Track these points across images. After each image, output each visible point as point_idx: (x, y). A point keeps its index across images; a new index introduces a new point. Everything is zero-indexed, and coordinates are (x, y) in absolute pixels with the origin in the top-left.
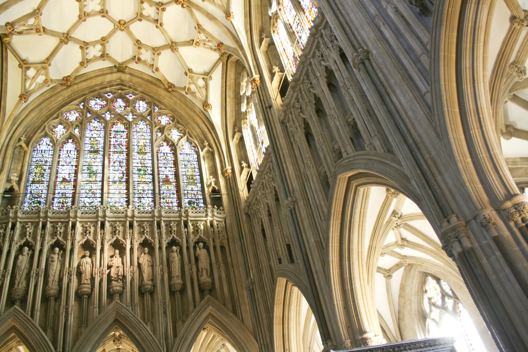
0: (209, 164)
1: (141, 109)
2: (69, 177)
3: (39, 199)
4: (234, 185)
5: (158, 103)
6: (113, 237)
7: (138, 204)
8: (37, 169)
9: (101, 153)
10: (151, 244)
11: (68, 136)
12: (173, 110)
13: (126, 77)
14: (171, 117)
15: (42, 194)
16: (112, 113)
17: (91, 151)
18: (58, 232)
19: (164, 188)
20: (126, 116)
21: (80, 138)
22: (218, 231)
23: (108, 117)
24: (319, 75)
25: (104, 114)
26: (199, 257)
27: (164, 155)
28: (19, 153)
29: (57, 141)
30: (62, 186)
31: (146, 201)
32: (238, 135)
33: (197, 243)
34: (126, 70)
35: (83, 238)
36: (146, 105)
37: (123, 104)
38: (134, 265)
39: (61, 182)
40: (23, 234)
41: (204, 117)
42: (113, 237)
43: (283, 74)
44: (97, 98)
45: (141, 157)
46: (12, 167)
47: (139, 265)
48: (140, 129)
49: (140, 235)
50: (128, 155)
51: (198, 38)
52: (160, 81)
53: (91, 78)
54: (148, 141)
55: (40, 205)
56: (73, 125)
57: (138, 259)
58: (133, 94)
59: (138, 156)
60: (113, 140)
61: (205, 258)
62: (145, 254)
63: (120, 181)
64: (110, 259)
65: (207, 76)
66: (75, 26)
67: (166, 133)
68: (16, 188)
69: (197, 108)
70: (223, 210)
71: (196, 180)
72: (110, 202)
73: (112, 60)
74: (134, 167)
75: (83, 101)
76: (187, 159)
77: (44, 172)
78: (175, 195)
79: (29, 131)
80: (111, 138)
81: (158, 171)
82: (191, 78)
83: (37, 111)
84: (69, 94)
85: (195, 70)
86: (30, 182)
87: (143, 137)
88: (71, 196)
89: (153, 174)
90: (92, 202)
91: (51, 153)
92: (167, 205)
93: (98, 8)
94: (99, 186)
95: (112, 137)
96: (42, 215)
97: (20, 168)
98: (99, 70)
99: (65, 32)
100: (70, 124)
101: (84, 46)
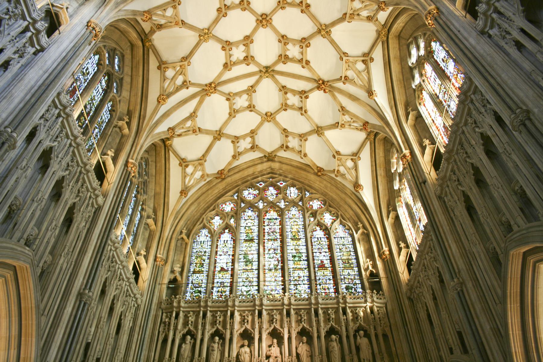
0: (364, 247)
1: (292, 195)
3: (199, 289)
4: (393, 267)
5: (308, 188)
6: (270, 326)
7: (294, 292)
9: (256, 241)
10: (309, 332)
11: (224, 227)
12: (324, 194)
13: (276, 165)
14: (322, 201)
15: (202, 283)
16: (265, 201)
18: (218, 322)
19: (319, 274)
20: (278, 204)
21: (236, 228)
22: (379, 318)
23: (261, 205)
24: (474, 143)
25: (257, 203)
26: (360, 347)
27: (318, 240)
28: (181, 245)
29: (214, 232)
30: (220, 275)
31: (302, 288)
32: (393, 214)
33: (357, 331)
34: (276, 159)
35: (242, 327)
36: (296, 191)
37: (274, 192)
38: (292, 355)
39: (220, 272)
40: (186, 324)
41: (356, 198)
42: (270, 326)
43: (434, 146)
44: (249, 188)
45: (295, 244)
46: (175, 258)
47: (298, 355)
49: (297, 324)
50: (281, 242)
51: (343, 120)
52: (309, 166)
53: (243, 170)
54: (301, 227)
55: (200, 294)
56: (228, 215)
57: (296, 348)
58: (284, 181)
60: (267, 228)
61: (367, 348)
62: (303, 343)
63: (275, 269)
64: (268, 349)
65: (356, 156)
66: (226, 123)
67: (318, 217)
68: (179, 278)
69: (348, 190)
70: (383, 295)
71: (352, 264)
72: (266, 290)
73: (262, 150)
74: (288, 254)
75: (237, 192)
76: (342, 243)
78: (332, 281)
79: (189, 224)
81: (313, 256)
82: (340, 160)
83: (196, 204)
84: (224, 186)
85: (342, 151)
86: (191, 272)
87: (296, 223)
88: (229, 285)
89: (308, 260)
90: (249, 291)
91: (209, 243)
92: (324, 291)
93: (246, 104)
94: (255, 274)
95: (266, 225)
96: (202, 304)
97: (182, 259)
98: (250, 161)
99: (218, 129)
100: (226, 215)
101: (236, 140)
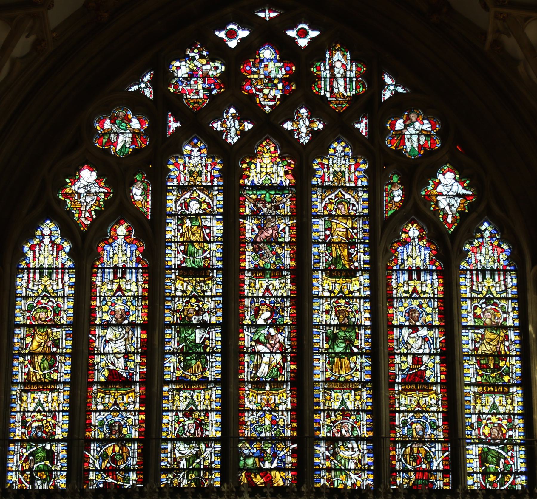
1: (340, 86)
2: (126, 366)
3: (48, 447)
8: (33, 338)
30: (109, 400)
48: (335, 173)
55: (52, 463)
59: (327, 283)
77: (54, 349)
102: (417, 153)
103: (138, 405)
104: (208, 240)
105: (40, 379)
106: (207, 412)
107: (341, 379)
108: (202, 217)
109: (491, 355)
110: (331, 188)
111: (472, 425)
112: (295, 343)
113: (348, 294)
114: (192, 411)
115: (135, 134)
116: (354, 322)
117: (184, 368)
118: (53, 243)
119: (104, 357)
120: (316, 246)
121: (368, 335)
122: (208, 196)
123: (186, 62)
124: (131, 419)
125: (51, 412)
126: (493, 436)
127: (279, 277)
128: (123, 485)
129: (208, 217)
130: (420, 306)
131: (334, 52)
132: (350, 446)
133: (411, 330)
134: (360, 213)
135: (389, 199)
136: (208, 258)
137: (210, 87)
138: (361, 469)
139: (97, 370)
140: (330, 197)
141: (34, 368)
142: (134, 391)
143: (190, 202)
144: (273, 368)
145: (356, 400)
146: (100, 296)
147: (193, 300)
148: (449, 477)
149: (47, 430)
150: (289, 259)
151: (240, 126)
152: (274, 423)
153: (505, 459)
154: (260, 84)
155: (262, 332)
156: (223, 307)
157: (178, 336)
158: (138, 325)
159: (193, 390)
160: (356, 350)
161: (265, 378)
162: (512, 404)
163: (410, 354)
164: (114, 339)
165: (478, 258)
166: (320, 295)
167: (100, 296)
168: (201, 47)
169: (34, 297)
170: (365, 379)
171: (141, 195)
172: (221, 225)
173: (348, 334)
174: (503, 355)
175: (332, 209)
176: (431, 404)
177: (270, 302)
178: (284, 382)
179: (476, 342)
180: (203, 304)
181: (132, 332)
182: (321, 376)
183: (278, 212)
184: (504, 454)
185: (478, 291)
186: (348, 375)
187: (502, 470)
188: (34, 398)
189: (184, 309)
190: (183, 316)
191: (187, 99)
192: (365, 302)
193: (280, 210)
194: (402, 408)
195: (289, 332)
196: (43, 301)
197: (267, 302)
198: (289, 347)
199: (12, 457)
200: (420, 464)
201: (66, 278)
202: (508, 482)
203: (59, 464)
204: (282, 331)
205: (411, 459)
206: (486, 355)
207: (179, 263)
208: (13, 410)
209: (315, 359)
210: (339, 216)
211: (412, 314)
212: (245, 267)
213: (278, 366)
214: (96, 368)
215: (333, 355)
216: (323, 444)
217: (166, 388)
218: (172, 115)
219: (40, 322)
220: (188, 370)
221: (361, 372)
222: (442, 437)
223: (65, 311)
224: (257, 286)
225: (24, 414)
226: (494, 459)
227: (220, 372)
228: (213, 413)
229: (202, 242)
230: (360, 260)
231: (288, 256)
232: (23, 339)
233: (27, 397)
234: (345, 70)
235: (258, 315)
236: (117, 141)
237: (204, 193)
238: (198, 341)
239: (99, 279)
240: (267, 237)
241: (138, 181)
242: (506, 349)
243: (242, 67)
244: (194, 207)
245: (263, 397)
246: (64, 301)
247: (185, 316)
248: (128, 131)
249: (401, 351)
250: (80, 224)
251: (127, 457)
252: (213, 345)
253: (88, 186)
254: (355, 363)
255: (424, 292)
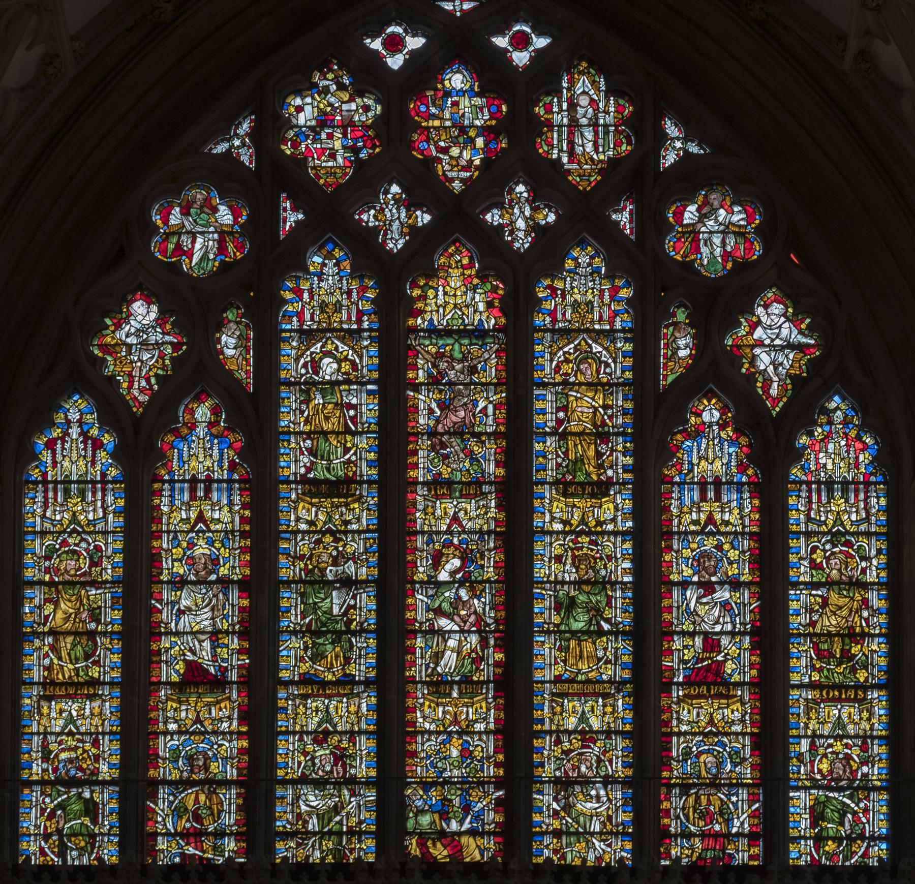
2: (214, 656)
3: (87, 795)
8: (57, 604)
17: (316, 482)
48: (576, 305)
55: (95, 822)
59: (558, 508)
77: (93, 626)
80: (416, 388)
102: (720, 267)
103: (235, 723)
104: (353, 429)
105: (70, 677)
106: (352, 735)
107: (580, 678)
108: (343, 387)
109: (838, 634)
110: (567, 334)
111: (800, 756)
112: (503, 613)
113: (595, 526)
114: (326, 733)
115: (223, 235)
116: (604, 577)
117: (314, 659)
118: (84, 434)
119: (176, 639)
120: (541, 439)
121: (627, 600)
122: (353, 349)
123: (313, 98)
124: (224, 747)
125: (91, 734)
126: (835, 775)
127: (475, 496)
128: (213, 859)
129: (352, 387)
130: (719, 547)
131: (576, 76)
132: (593, 793)
133: (701, 591)
134: (618, 379)
135: (670, 353)
136: (353, 462)
137: (355, 145)
138: (611, 833)
139: (167, 662)
140: (566, 349)
141: (60, 659)
142: (229, 698)
143: (321, 359)
144: (464, 659)
145: (605, 714)
146: (168, 532)
147: (328, 539)
148: (759, 846)
149: (85, 766)
150: (492, 466)
151: (409, 218)
152: (466, 753)
153: (855, 813)
154: (443, 137)
155: (447, 594)
156: (380, 550)
157: (302, 602)
158: (233, 582)
159: (329, 697)
160: (606, 627)
161: (451, 677)
162: (869, 719)
163: (700, 633)
164: (194, 608)
165: (822, 461)
166: (546, 528)
167: (168, 532)
168: (340, 68)
169: (56, 532)
170: (621, 677)
171: (235, 348)
172: (376, 401)
173: (593, 599)
174: (858, 634)
175: (570, 371)
176: (733, 721)
177: (460, 541)
178: (483, 682)
179: (812, 611)
180: (344, 546)
181: (224, 594)
182: (547, 671)
183: (475, 378)
184: (853, 805)
185: (820, 521)
186: (593, 670)
187: (848, 832)
188: (60, 709)
189: (311, 555)
190: (310, 567)
191: (314, 168)
192: (624, 541)
193: (479, 373)
194: (684, 728)
195: (492, 595)
196: (70, 540)
197: (456, 541)
198: (492, 621)
199: (27, 810)
200: (711, 823)
201: (110, 499)
202: (857, 853)
203: (106, 823)
204: (481, 594)
205: (696, 815)
206: (830, 635)
207: (303, 470)
208: (27, 730)
209: (537, 642)
210: (580, 384)
211: (704, 561)
212: (417, 478)
213: (474, 655)
214: (164, 658)
215: (567, 635)
216: (548, 789)
217: (282, 694)
218: (287, 198)
219: (67, 577)
220: (320, 661)
221: (615, 664)
222: (749, 776)
223: (108, 558)
224: (438, 512)
225: (45, 738)
226: (836, 814)
227: (374, 665)
228: (363, 738)
229: (342, 433)
230: (617, 465)
231: (492, 458)
232: (40, 607)
233: (50, 708)
234: (596, 110)
235: (439, 565)
236: (193, 247)
237: (345, 344)
238: (336, 611)
239: (165, 500)
240: (455, 423)
241: (230, 321)
242: (864, 624)
243: (412, 106)
244: (329, 367)
245: (447, 708)
246: (106, 540)
247: (314, 567)
248: (212, 229)
249: (684, 627)
250: (131, 403)
251: (220, 812)
252: (363, 619)
253: (143, 331)
254: (605, 649)
255: (727, 523)
